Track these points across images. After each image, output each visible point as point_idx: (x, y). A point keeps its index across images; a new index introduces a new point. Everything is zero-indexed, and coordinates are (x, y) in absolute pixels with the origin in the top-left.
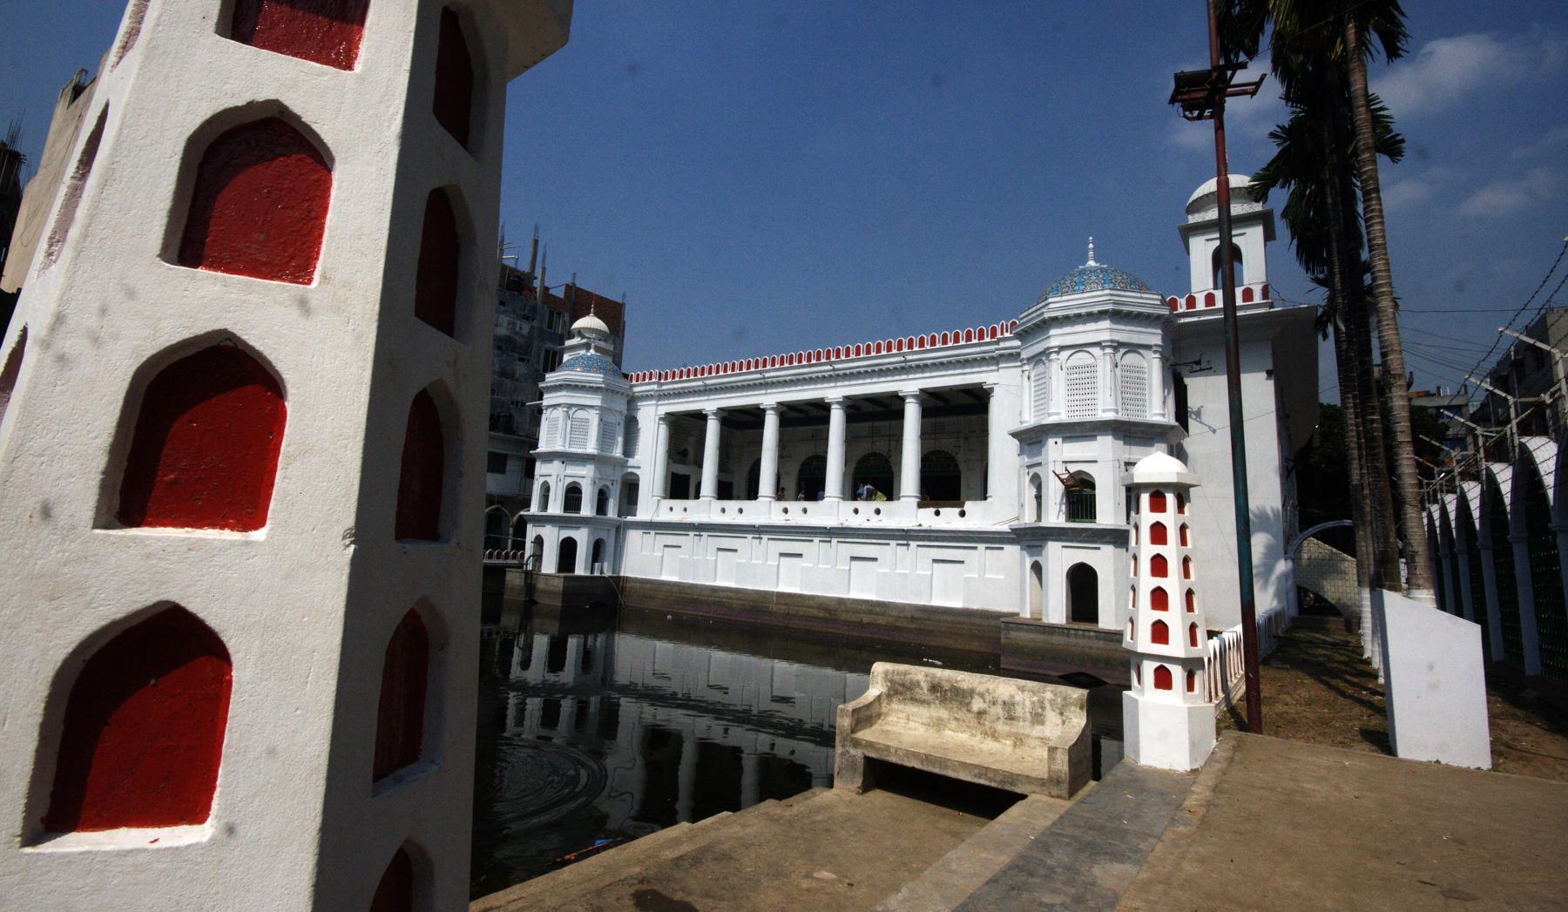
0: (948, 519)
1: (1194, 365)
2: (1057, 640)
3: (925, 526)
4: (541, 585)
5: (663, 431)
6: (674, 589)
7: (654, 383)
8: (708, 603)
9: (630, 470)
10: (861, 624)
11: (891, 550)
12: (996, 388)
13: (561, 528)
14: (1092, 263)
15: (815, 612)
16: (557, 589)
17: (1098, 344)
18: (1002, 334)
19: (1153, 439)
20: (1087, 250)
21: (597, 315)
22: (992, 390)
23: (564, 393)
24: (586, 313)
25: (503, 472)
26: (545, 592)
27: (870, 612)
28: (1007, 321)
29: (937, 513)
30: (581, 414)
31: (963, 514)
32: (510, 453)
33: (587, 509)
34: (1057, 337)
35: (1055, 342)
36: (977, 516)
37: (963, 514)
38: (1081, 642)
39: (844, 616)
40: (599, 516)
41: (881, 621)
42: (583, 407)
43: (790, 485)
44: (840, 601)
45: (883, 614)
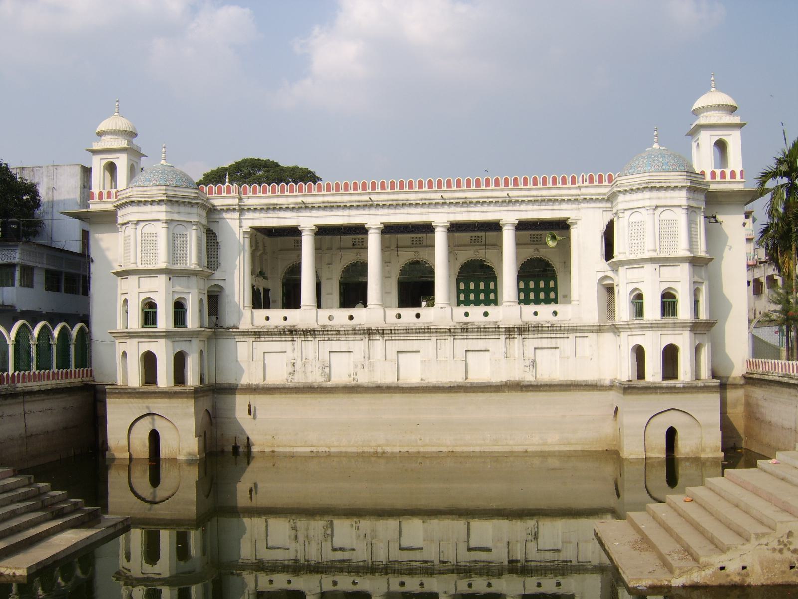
1: (713, 218)
7: (233, 197)
12: (579, 222)
14: (656, 146)
18: (583, 183)
19: (703, 266)
22: (574, 223)
25: (32, 286)
28: (586, 175)
32: (37, 264)
33: (192, 321)
36: (566, 313)
43: (332, 291)
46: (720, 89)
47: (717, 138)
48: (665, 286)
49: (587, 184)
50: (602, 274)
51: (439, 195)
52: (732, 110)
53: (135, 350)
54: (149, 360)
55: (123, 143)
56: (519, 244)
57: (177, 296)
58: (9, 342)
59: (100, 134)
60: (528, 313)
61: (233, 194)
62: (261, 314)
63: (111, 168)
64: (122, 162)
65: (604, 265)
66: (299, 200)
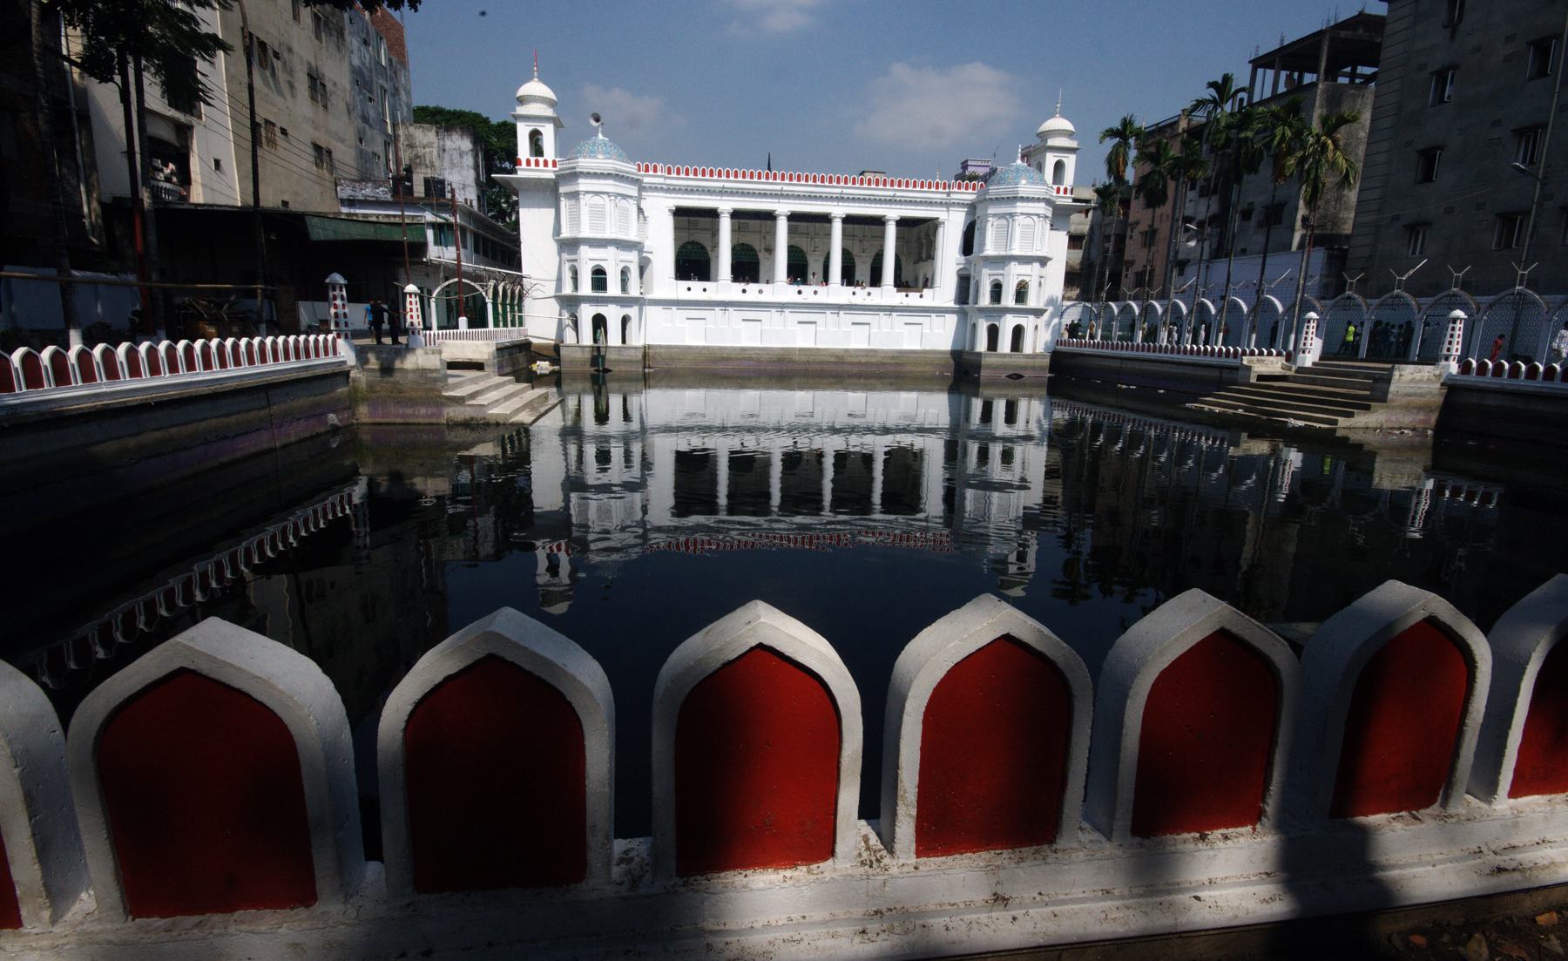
0: (913, 299)
2: (1007, 360)
3: (905, 304)
4: (611, 356)
5: (669, 222)
6: (704, 351)
8: (737, 359)
9: (645, 255)
10: (860, 363)
11: (829, 316)
13: (622, 306)
15: (829, 359)
16: (635, 358)
17: (1038, 215)
20: (1017, 153)
21: (543, 80)
23: (611, 182)
24: (529, 79)
26: (618, 362)
27: (867, 356)
29: (907, 296)
30: (623, 203)
31: (921, 296)
34: (1021, 207)
35: (1019, 210)
36: (928, 298)
37: (921, 296)
38: (1015, 360)
39: (849, 360)
40: (596, 294)
41: (873, 360)
42: (624, 197)
44: (847, 351)
45: (875, 356)
46: (1064, 116)
47: (1057, 159)
48: (1021, 278)
49: (956, 190)
50: (962, 266)
51: (839, 191)
52: (1070, 135)
53: (587, 313)
54: (599, 322)
55: (549, 112)
56: (899, 238)
57: (624, 264)
58: (487, 300)
59: (522, 101)
60: (899, 298)
61: (659, 173)
62: (685, 284)
63: (535, 137)
64: (548, 132)
65: (962, 259)
66: (721, 185)
